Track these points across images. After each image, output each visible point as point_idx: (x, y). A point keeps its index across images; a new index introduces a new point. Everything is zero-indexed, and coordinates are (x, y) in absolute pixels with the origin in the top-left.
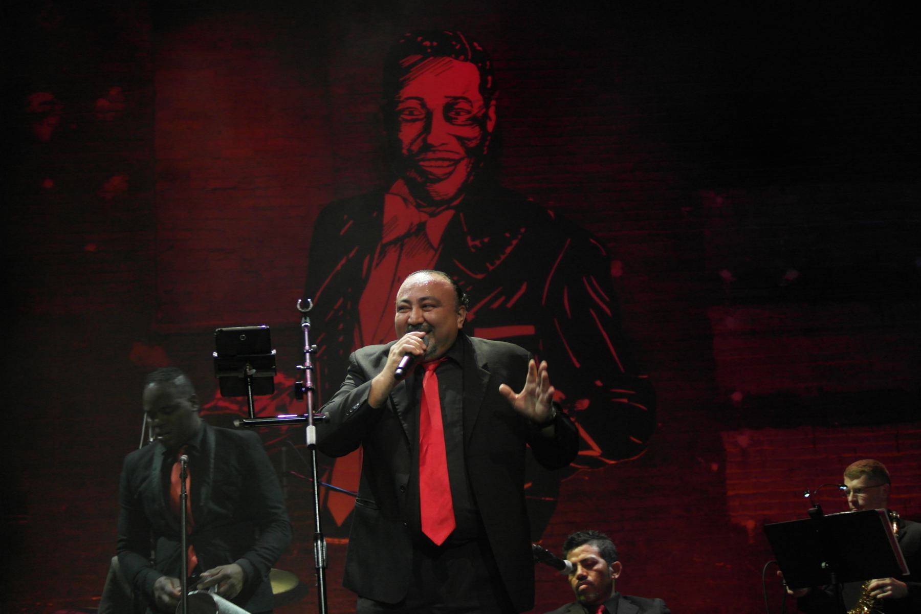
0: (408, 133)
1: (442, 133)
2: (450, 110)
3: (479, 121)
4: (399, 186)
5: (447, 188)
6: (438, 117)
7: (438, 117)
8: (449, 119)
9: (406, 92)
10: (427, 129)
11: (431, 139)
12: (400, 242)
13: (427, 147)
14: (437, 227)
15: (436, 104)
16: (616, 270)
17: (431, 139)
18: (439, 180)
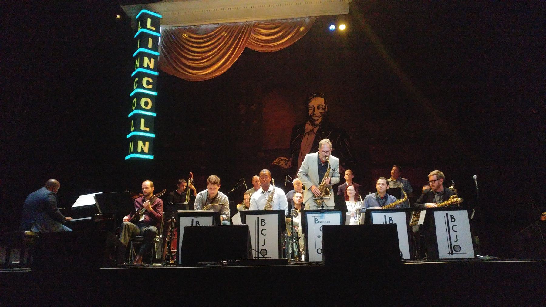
0: (310, 112)
1: (317, 112)
2: (319, 107)
3: (324, 109)
4: (309, 122)
5: (318, 122)
6: (316, 108)
7: (316, 108)
8: (318, 109)
9: (310, 104)
10: (314, 111)
11: (315, 113)
12: (308, 133)
13: (314, 114)
14: (316, 130)
15: (316, 106)
16: (351, 138)
17: (315, 113)
18: (316, 121)
